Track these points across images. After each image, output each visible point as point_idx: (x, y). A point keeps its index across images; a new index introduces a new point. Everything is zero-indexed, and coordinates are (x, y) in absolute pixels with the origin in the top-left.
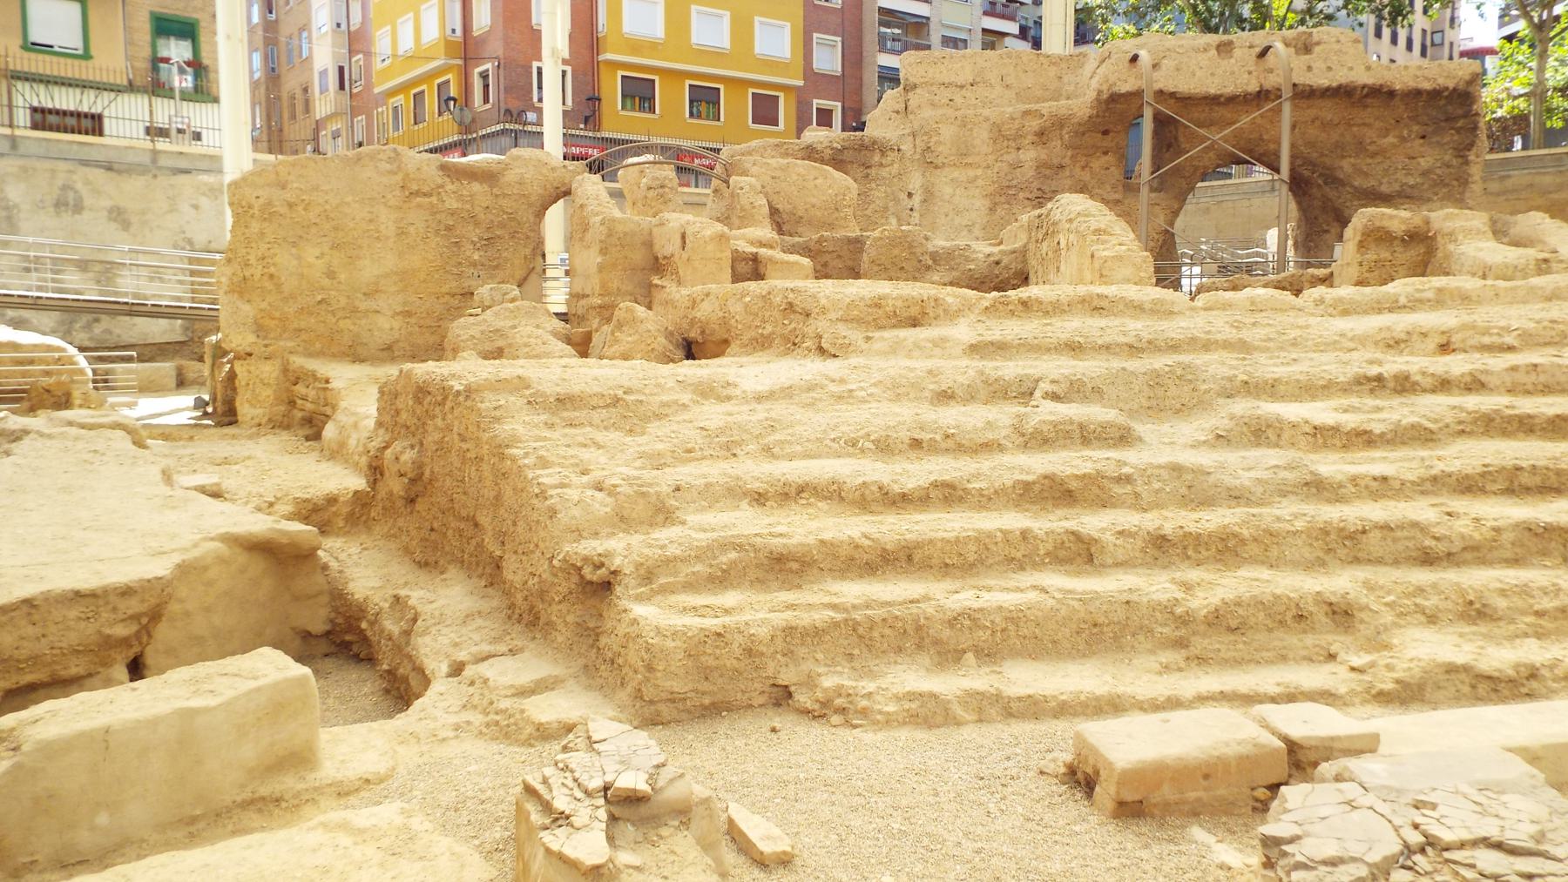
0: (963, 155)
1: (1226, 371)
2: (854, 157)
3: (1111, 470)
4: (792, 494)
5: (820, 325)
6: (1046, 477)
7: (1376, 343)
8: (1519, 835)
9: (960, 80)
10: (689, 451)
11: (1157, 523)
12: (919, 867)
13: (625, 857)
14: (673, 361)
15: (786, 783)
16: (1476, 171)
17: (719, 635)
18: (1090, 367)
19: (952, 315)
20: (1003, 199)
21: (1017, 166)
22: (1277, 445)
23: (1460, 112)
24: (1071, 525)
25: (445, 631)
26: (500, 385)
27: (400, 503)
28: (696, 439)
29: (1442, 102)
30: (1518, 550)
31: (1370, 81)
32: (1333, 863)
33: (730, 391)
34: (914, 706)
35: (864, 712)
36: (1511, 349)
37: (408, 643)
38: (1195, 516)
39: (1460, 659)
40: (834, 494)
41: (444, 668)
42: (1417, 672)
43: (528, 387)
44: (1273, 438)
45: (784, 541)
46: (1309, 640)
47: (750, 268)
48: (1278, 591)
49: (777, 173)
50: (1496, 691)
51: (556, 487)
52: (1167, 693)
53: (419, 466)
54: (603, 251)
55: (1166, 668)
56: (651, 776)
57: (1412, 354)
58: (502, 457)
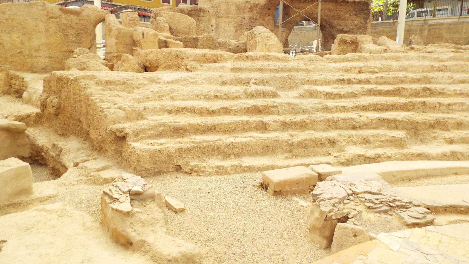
0: (228, 13)
1: (303, 77)
2: (195, 13)
3: (272, 104)
4: (180, 111)
5: (187, 62)
6: (253, 106)
7: (343, 70)
8: (375, 190)
10: (148, 98)
11: (284, 119)
12: (220, 211)
13: (136, 210)
14: (141, 72)
15: (181, 191)
16: (369, 25)
17: (159, 151)
18: (265, 76)
19: (226, 60)
20: (239, 28)
21: (243, 18)
22: (316, 98)
23: (365, 8)
24: (261, 119)
25: (71, 154)
26: (86, 77)
27: (52, 116)
28: (150, 95)
29: (361, 5)
30: (377, 125)
32: (330, 199)
33: (160, 81)
34: (217, 169)
35: (203, 172)
36: (377, 72)
37: (59, 158)
38: (294, 117)
39: (361, 153)
40: (192, 111)
41: (72, 164)
42: (351, 157)
43: (96, 78)
44: (315, 96)
45: (178, 124)
46: (324, 150)
47: (164, 44)
48: (316, 137)
49: (171, 17)
50: (370, 161)
51: (106, 108)
52: (287, 164)
53: (59, 104)
54: (117, 38)
55: (287, 158)
56: (143, 187)
57: (351, 73)
58: (88, 100)
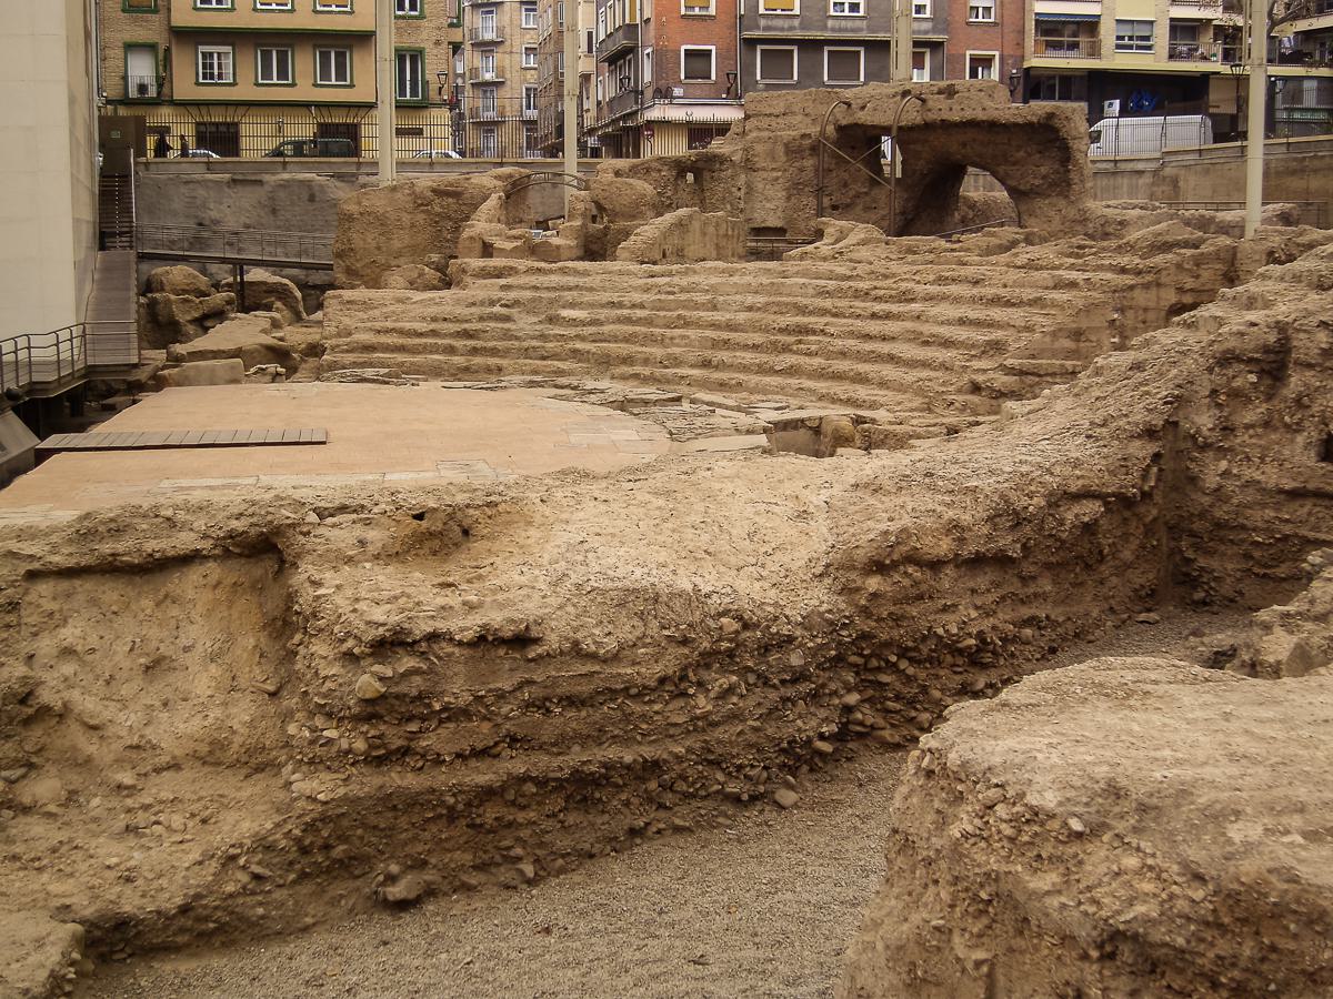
4: (388, 331)
9: (776, 112)
21: (801, 170)
31: (985, 118)
40: (401, 332)
